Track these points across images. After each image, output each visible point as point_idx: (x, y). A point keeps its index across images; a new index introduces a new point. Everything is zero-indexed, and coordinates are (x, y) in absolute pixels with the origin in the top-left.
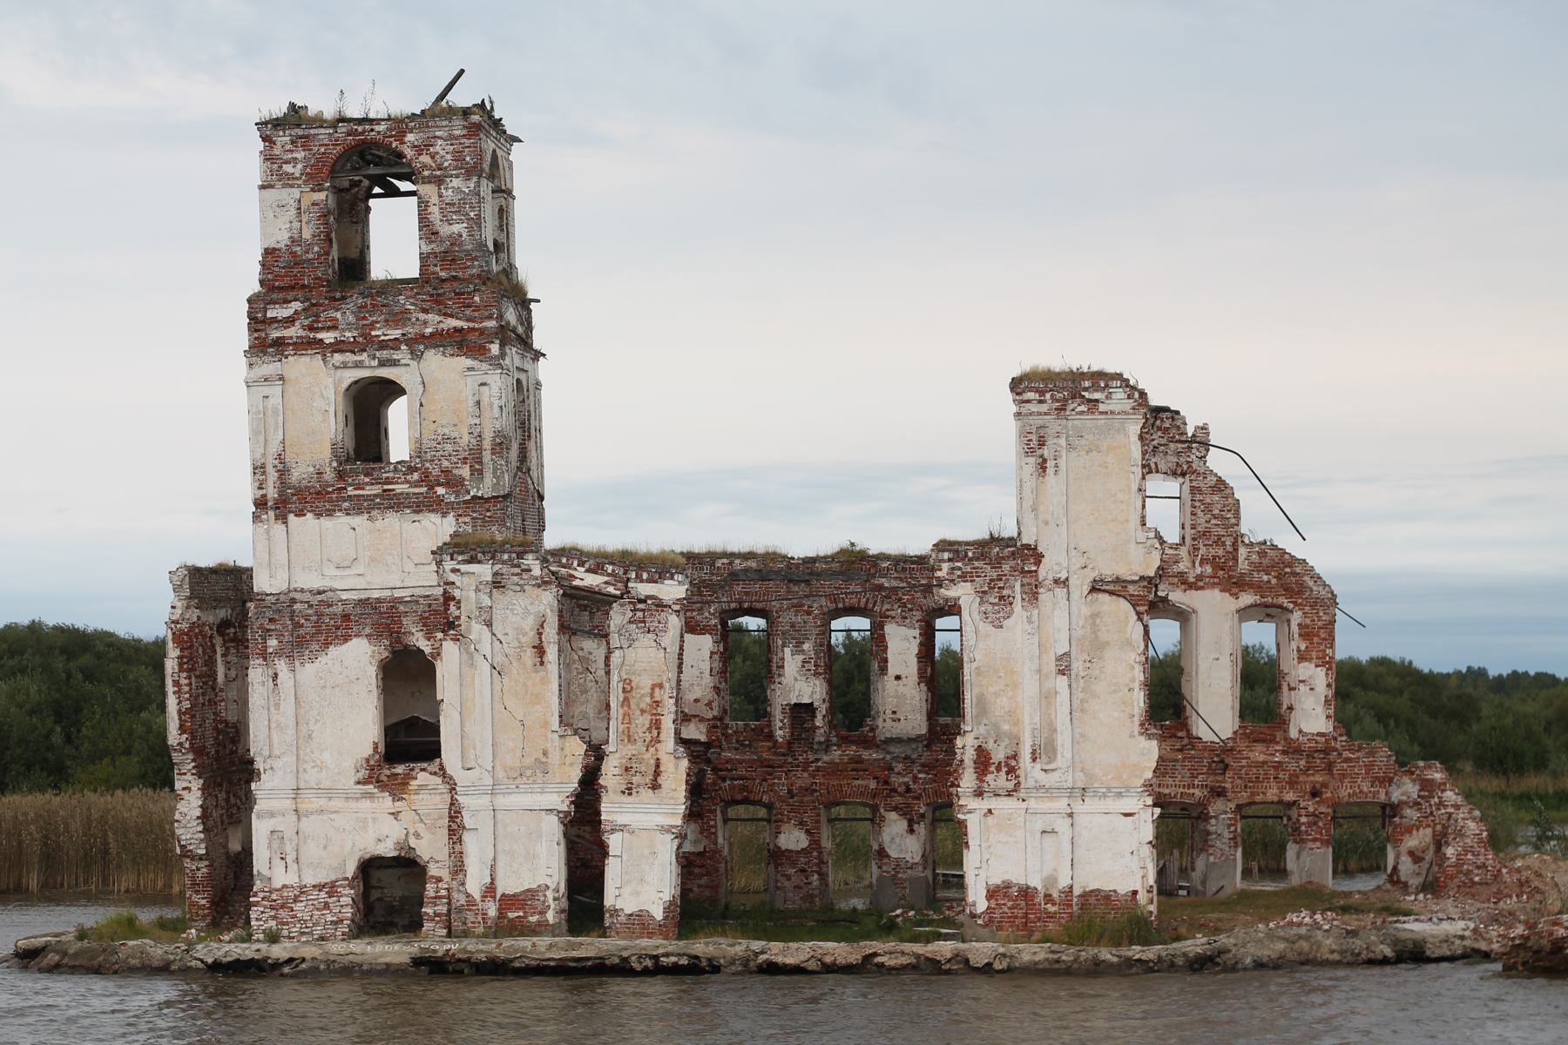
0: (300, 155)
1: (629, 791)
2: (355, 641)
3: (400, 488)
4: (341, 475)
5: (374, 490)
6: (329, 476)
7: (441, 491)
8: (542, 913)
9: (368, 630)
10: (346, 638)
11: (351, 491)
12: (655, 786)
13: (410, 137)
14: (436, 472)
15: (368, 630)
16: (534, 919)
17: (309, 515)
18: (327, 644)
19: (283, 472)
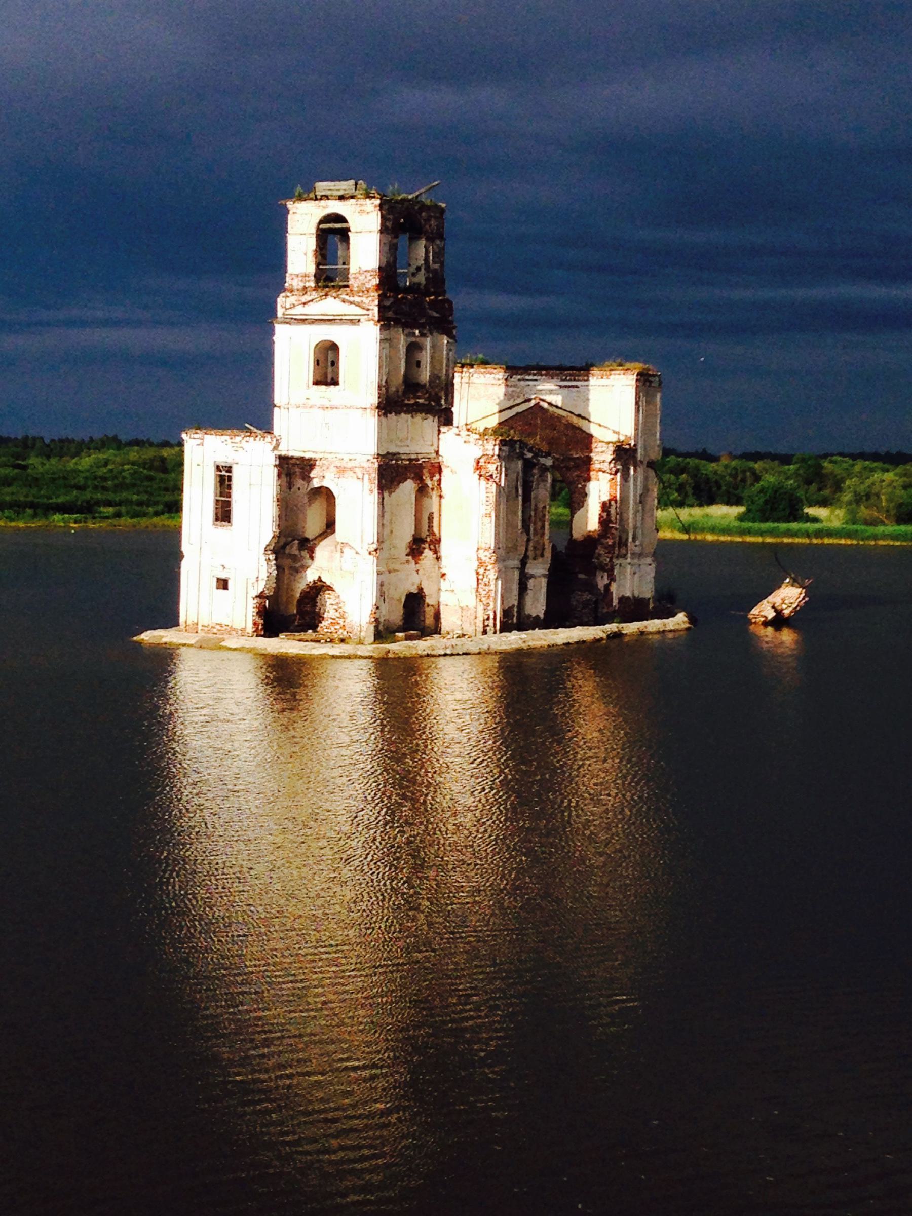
0: (391, 217)
1: (534, 559)
2: (409, 480)
3: (421, 401)
4: (405, 393)
5: (412, 402)
6: (400, 393)
7: (433, 404)
8: (512, 619)
9: (413, 475)
10: (406, 480)
11: (406, 402)
12: (542, 556)
13: (423, 214)
14: (433, 393)
15: (413, 475)
16: (510, 622)
17: (393, 414)
18: (398, 484)
19: (387, 390)
